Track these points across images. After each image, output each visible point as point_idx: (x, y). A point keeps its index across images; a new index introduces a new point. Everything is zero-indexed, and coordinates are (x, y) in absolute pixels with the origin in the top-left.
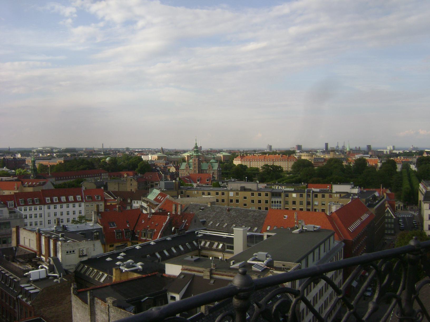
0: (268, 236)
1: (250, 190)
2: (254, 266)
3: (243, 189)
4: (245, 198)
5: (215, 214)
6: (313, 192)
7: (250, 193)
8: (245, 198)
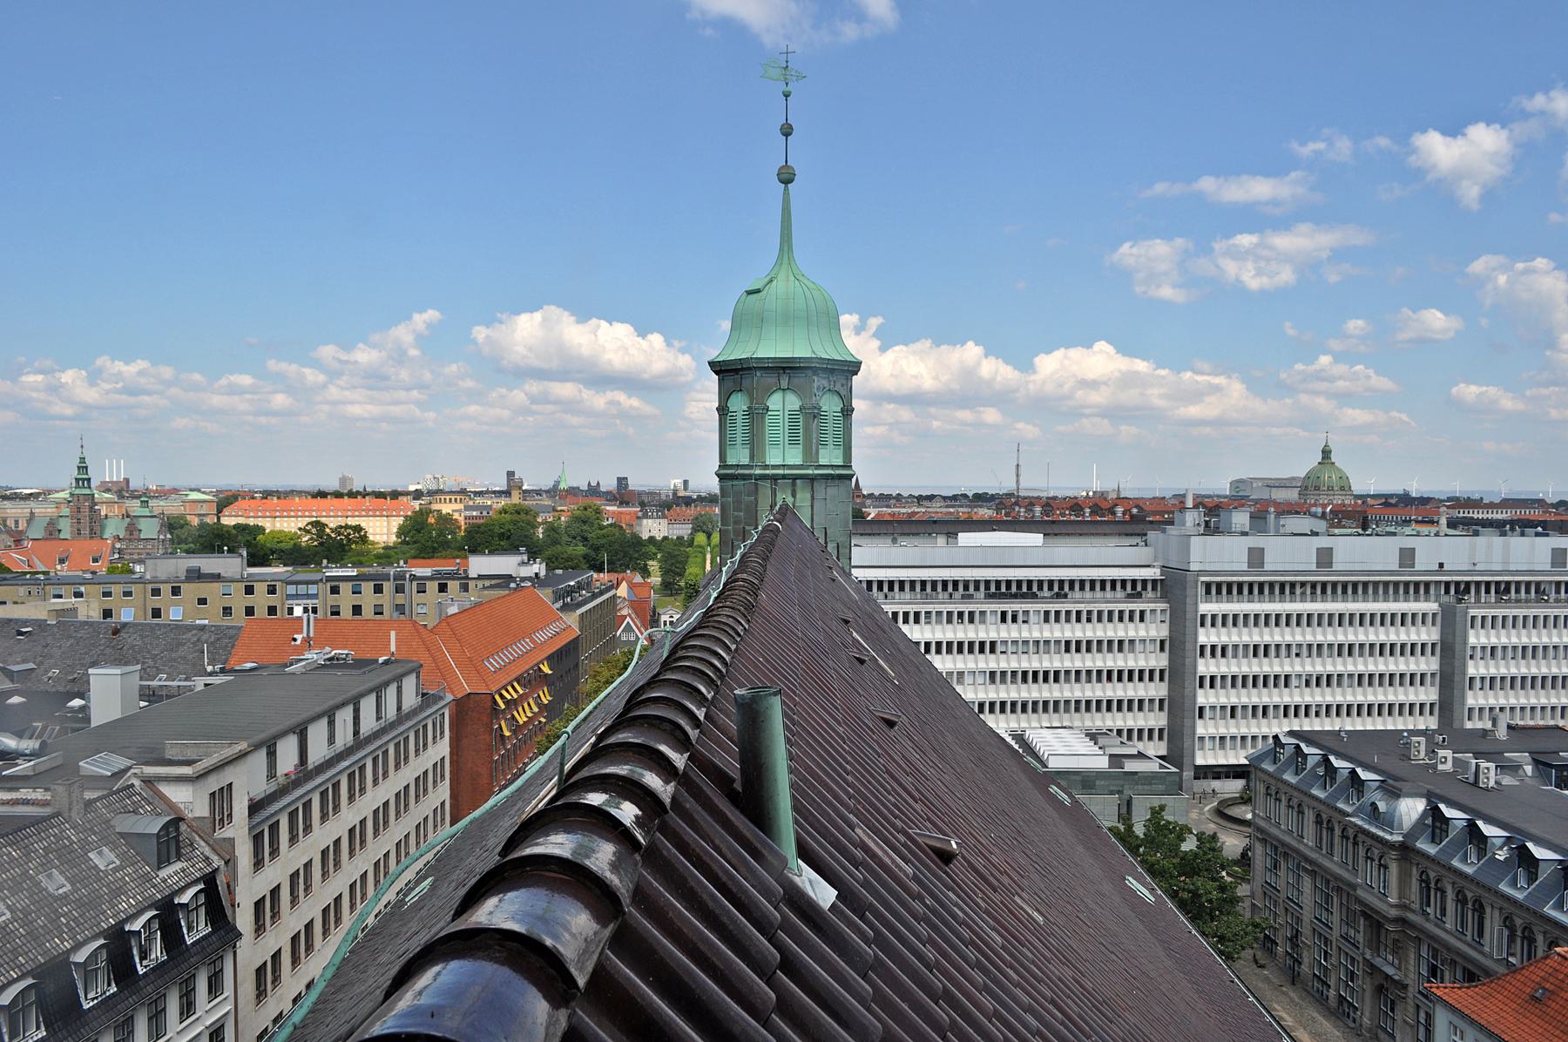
0: (206, 685)
1: (216, 578)
2: (87, 763)
3: (196, 576)
4: (202, 601)
5: (72, 645)
6: (414, 578)
7: (218, 587)
8: (202, 601)
